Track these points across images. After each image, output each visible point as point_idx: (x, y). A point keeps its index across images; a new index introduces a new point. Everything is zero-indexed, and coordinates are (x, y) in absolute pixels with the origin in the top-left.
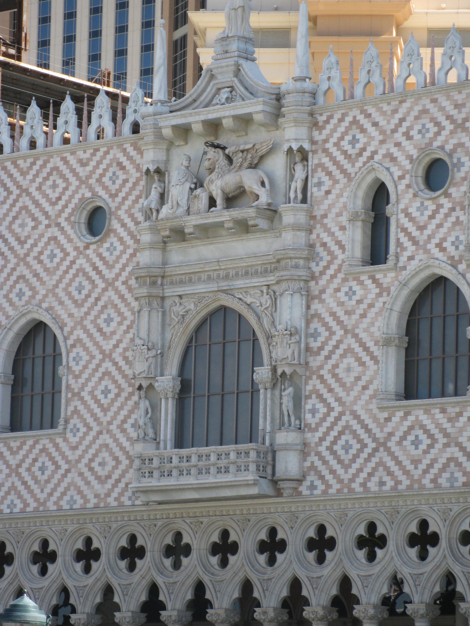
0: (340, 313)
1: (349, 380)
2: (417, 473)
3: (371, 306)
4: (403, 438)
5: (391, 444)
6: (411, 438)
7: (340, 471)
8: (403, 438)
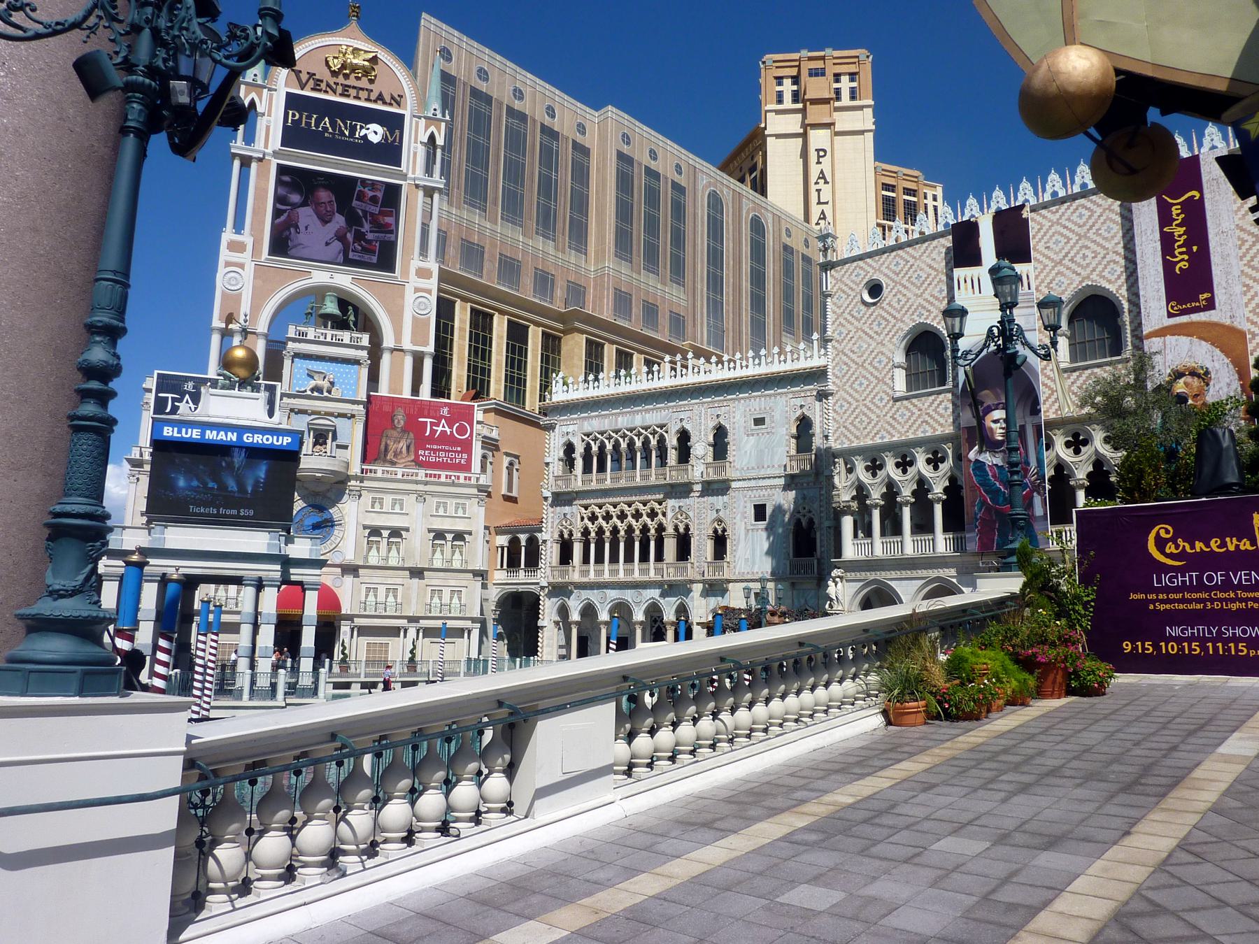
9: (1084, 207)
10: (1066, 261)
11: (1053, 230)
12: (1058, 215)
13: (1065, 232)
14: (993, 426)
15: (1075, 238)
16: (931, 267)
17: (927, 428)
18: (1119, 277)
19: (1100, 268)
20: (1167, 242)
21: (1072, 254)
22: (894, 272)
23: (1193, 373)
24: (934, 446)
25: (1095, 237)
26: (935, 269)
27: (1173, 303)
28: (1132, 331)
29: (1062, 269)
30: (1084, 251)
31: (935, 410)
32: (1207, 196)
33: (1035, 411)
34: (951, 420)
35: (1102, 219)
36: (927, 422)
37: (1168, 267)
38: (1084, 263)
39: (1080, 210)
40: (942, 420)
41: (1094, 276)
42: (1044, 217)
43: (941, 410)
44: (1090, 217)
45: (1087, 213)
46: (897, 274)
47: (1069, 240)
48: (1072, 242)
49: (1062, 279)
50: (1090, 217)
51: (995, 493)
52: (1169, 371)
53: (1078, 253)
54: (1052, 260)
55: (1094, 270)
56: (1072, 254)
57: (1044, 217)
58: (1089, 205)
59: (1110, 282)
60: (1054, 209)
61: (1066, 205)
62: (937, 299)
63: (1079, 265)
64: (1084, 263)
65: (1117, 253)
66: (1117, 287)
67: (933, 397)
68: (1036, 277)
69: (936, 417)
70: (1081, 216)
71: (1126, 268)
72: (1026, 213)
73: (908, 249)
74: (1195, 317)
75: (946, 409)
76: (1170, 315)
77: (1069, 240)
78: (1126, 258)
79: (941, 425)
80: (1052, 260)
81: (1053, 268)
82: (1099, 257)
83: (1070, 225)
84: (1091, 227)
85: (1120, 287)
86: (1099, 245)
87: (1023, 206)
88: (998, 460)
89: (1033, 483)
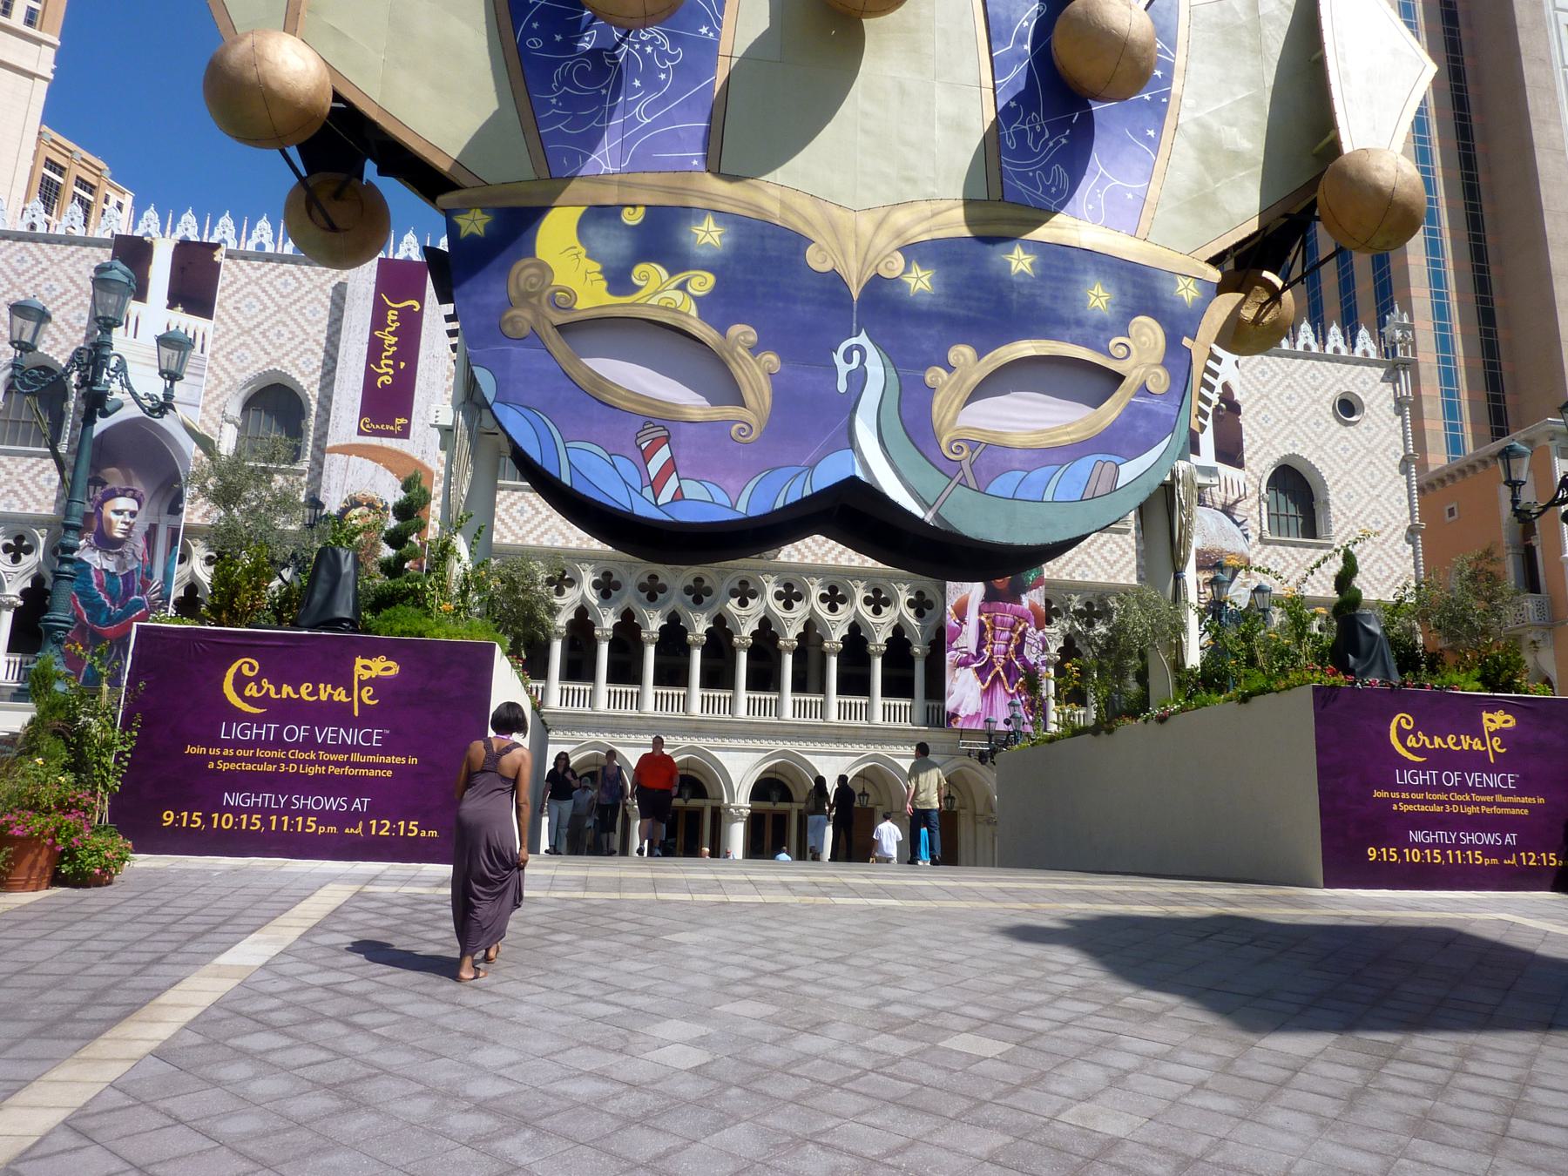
9: (292, 274)
10: (256, 333)
11: (249, 289)
12: (258, 274)
13: (263, 296)
14: (114, 517)
15: (273, 308)
16: (72, 281)
17: (15, 501)
18: (314, 372)
19: (294, 354)
20: (375, 349)
21: (265, 326)
22: (15, 270)
23: (371, 506)
24: (19, 529)
25: (297, 315)
26: (78, 287)
27: (367, 420)
28: (315, 440)
29: (249, 341)
30: (280, 327)
31: (33, 479)
32: (426, 311)
33: (175, 509)
34: (54, 497)
35: (310, 297)
36: (16, 493)
37: (370, 377)
38: (278, 342)
39: (287, 276)
40: (40, 495)
41: (285, 362)
42: (241, 270)
43: (41, 480)
44: (296, 289)
45: (294, 284)
46: (19, 275)
47: (266, 308)
48: (268, 312)
49: (247, 353)
50: (296, 289)
51: (95, 608)
52: (345, 496)
53: (272, 327)
54: (240, 326)
55: (287, 354)
56: (265, 326)
57: (241, 270)
58: (298, 274)
59: (302, 373)
60: (256, 264)
61: (271, 265)
62: (71, 326)
63: (271, 342)
64: (278, 342)
65: (318, 344)
66: (308, 382)
67: (34, 460)
68: (215, 341)
69: (33, 488)
70: (286, 284)
71: (324, 364)
72: (219, 256)
73: (44, 246)
74: (387, 442)
75: (50, 480)
76: (361, 432)
77: (266, 308)
78: (326, 351)
79: (38, 501)
80: (240, 326)
81: (238, 336)
82: (297, 341)
83: (271, 291)
84: (295, 302)
85: (313, 383)
86: (299, 325)
87: (216, 246)
88: (110, 565)
89: (152, 602)
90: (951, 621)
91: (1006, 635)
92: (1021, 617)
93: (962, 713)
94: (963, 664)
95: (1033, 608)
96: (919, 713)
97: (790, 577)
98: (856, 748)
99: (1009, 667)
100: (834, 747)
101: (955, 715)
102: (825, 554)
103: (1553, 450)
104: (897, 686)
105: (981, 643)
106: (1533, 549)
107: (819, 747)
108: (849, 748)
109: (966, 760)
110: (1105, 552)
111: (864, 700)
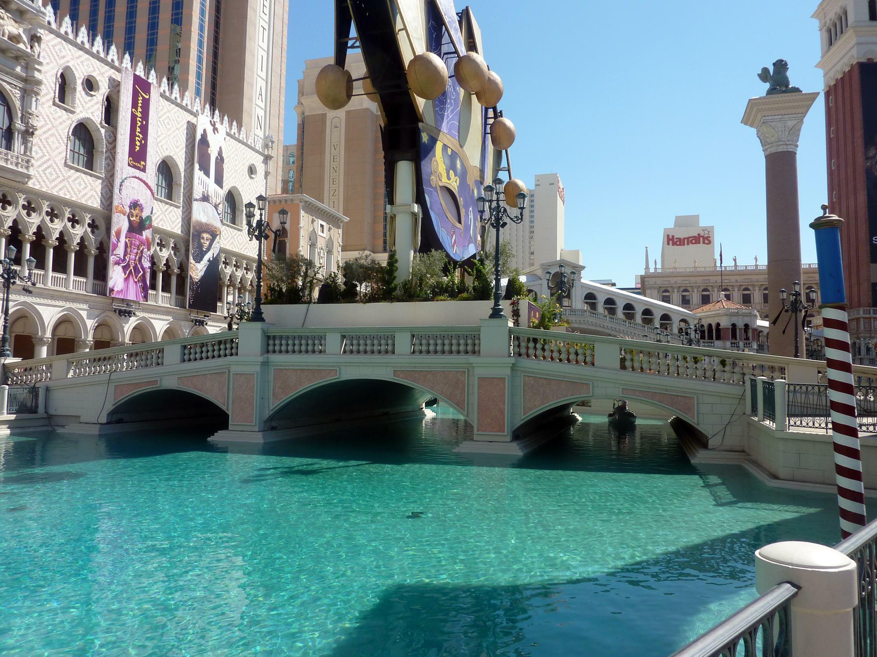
0: (51, 117)
1: (54, 147)
2: (80, 196)
3: (64, 121)
4: (75, 180)
5: (70, 180)
6: (78, 181)
7: (48, 183)
8: (75, 180)
90: (113, 239)
91: (135, 251)
92: (142, 243)
93: (116, 289)
94: (117, 263)
95: (147, 239)
96: (90, 288)
97: (32, 196)
98: (61, 303)
99: (135, 268)
100: (49, 302)
101: (112, 290)
102: (52, 188)
103: (301, 207)
104: (80, 271)
105: (125, 255)
106: (285, 243)
107: (42, 301)
108: (57, 303)
109: (111, 314)
110: (171, 215)
111: (63, 276)
